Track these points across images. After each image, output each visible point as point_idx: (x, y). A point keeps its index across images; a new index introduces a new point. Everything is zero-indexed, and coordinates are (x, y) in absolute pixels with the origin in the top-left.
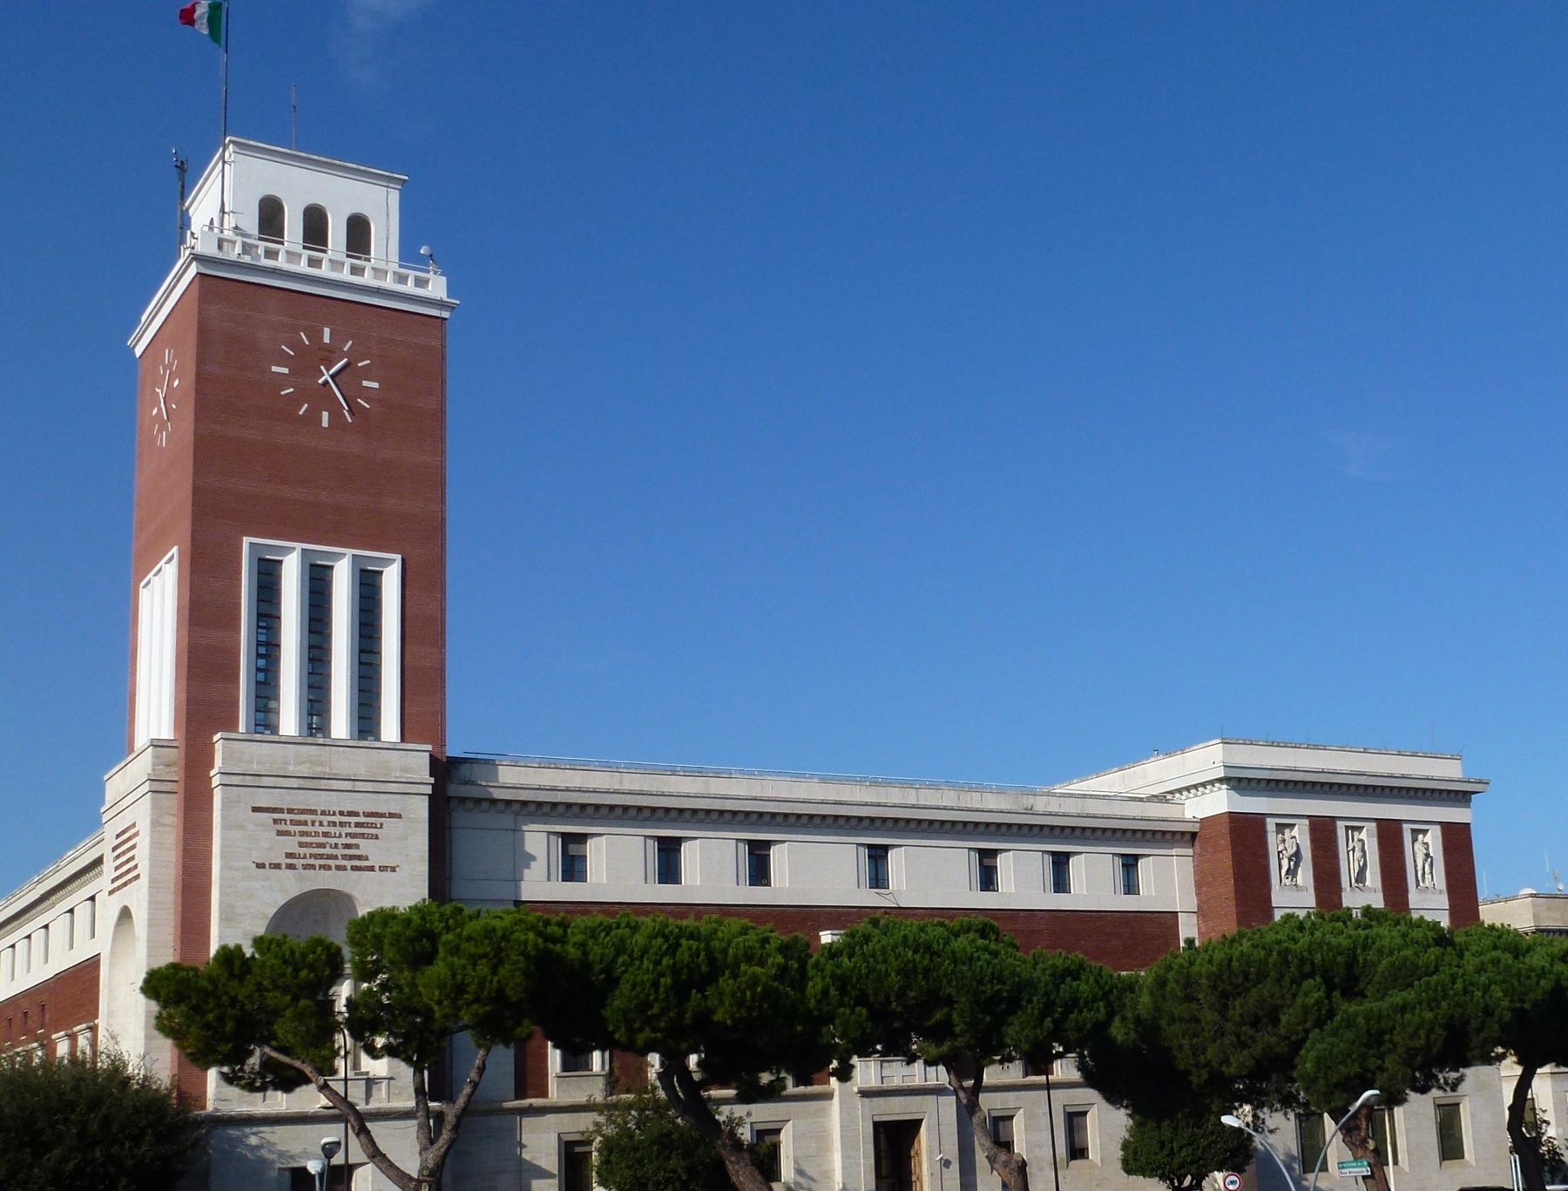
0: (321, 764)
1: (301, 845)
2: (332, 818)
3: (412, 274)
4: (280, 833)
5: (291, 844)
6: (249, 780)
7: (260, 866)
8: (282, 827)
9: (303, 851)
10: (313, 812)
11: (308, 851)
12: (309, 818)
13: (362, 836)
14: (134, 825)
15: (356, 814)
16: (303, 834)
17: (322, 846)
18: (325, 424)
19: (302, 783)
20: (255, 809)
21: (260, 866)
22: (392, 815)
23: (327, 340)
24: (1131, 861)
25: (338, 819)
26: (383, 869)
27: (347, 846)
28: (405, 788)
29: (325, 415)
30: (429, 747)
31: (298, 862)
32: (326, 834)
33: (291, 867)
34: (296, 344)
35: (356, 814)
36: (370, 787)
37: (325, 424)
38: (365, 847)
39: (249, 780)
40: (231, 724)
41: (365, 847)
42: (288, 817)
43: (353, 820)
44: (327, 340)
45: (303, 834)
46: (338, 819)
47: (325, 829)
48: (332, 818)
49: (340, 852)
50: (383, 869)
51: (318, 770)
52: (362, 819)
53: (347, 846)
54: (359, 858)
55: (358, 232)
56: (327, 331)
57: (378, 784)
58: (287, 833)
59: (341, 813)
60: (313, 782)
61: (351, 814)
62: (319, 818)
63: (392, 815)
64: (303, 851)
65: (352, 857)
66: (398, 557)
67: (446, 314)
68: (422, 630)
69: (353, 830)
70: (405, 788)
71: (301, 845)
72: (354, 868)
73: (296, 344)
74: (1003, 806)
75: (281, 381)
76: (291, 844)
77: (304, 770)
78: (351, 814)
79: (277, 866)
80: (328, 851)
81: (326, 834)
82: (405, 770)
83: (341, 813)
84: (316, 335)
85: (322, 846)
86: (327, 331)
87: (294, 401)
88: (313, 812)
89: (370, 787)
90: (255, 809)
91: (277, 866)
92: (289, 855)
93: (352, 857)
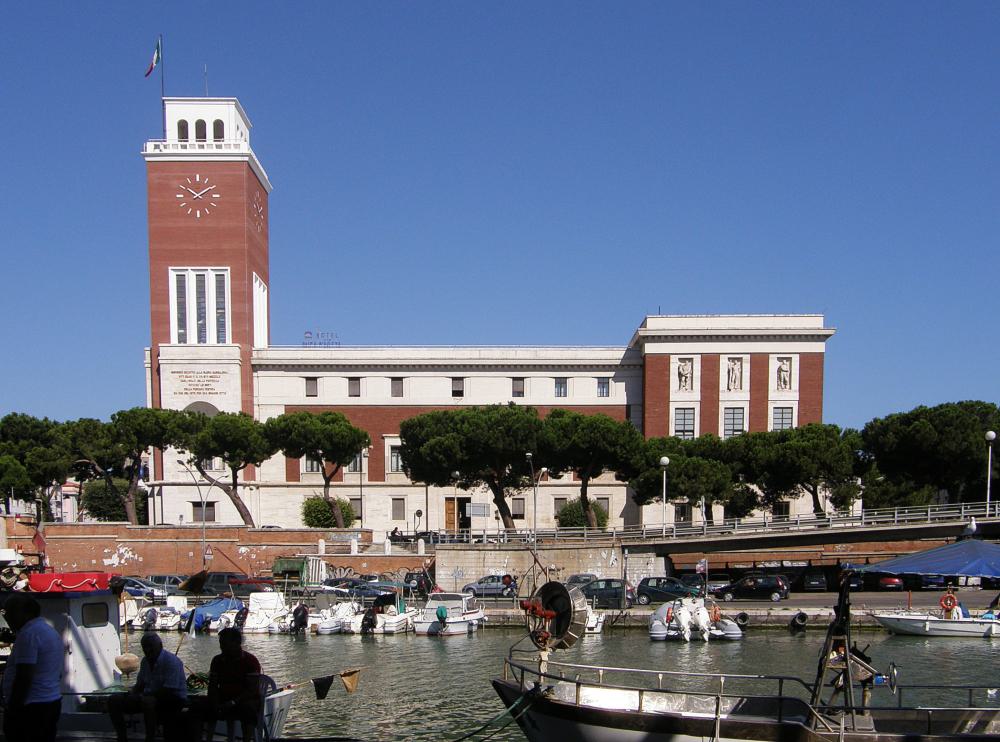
0: (197, 354)
5: (186, 385)
6: (170, 362)
8: (183, 379)
10: (194, 372)
11: (192, 387)
18: (198, 216)
22: (224, 372)
24: (606, 381)
29: (198, 212)
34: (186, 185)
36: (215, 362)
39: (170, 362)
40: (167, 339)
49: (204, 387)
55: (219, 127)
56: (198, 176)
57: (219, 361)
60: (193, 361)
63: (224, 372)
66: (229, 268)
74: (528, 357)
76: (186, 385)
78: (208, 372)
82: (228, 354)
84: (193, 178)
87: (186, 208)
88: (194, 372)
89: (215, 362)
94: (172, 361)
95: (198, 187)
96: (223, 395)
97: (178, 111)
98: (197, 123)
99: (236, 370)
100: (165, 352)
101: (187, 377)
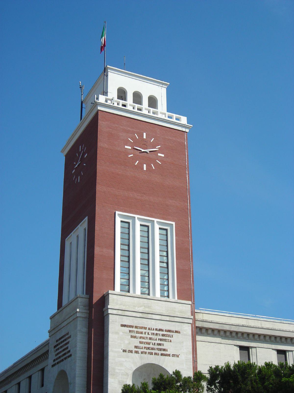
0: (149, 307)
1: (141, 343)
2: (153, 332)
3: (175, 116)
4: (132, 337)
5: (136, 342)
6: (120, 312)
7: (124, 351)
8: (133, 334)
9: (141, 345)
10: (145, 328)
11: (143, 345)
12: (144, 331)
13: (165, 340)
14: (68, 334)
15: (162, 330)
16: (140, 338)
17: (149, 344)
18: (145, 169)
19: (140, 315)
20: (123, 326)
21: (124, 351)
22: (176, 332)
23: (145, 137)
25: (155, 332)
26: (174, 355)
27: (160, 344)
28: (181, 320)
29: (145, 165)
30: (190, 302)
31: (140, 351)
32: (150, 339)
33: (137, 352)
34: (134, 138)
35: (162, 330)
36: (168, 318)
37: (145, 169)
38: (166, 345)
39: (120, 312)
41: (166, 345)
42: (136, 330)
43: (161, 333)
44: (145, 137)
45: (140, 338)
46: (155, 332)
47: (150, 336)
48: (153, 332)
49: (156, 347)
50: (174, 355)
51: (147, 310)
52: (164, 333)
53: (160, 344)
54: (164, 350)
56: (145, 134)
58: (135, 337)
59: (156, 329)
60: (145, 315)
61: (160, 330)
62: (147, 331)
63: (176, 332)
64: (141, 345)
65: (160, 350)
67: (187, 130)
68: (184, 253)
69: (161, 337)
70: (181, 320)
71: (141, 343)
72: (162, 355)
73: (134, 138)
75: (127, 152)
76: (136, 342)
77: (141, 310)
78: (160, 330)
79: (131, 352)
80: (151, 346)
81: (150, 339)
83: (156, 329)
85: (149, 344)
86: (145, 134)
87: (134, 159)
88: (145, 328)
89: (168, 318)
90: (123, 326)
91: (131, 352)
92: (136, 347)
93: (160, 350)
94: (123, 312)
95: (145, 144)
96: (175, 358)
97: (116, 80)
98: (133, 93)
99: (187, 330)
100: (115, 302)
101: (137, 332)
